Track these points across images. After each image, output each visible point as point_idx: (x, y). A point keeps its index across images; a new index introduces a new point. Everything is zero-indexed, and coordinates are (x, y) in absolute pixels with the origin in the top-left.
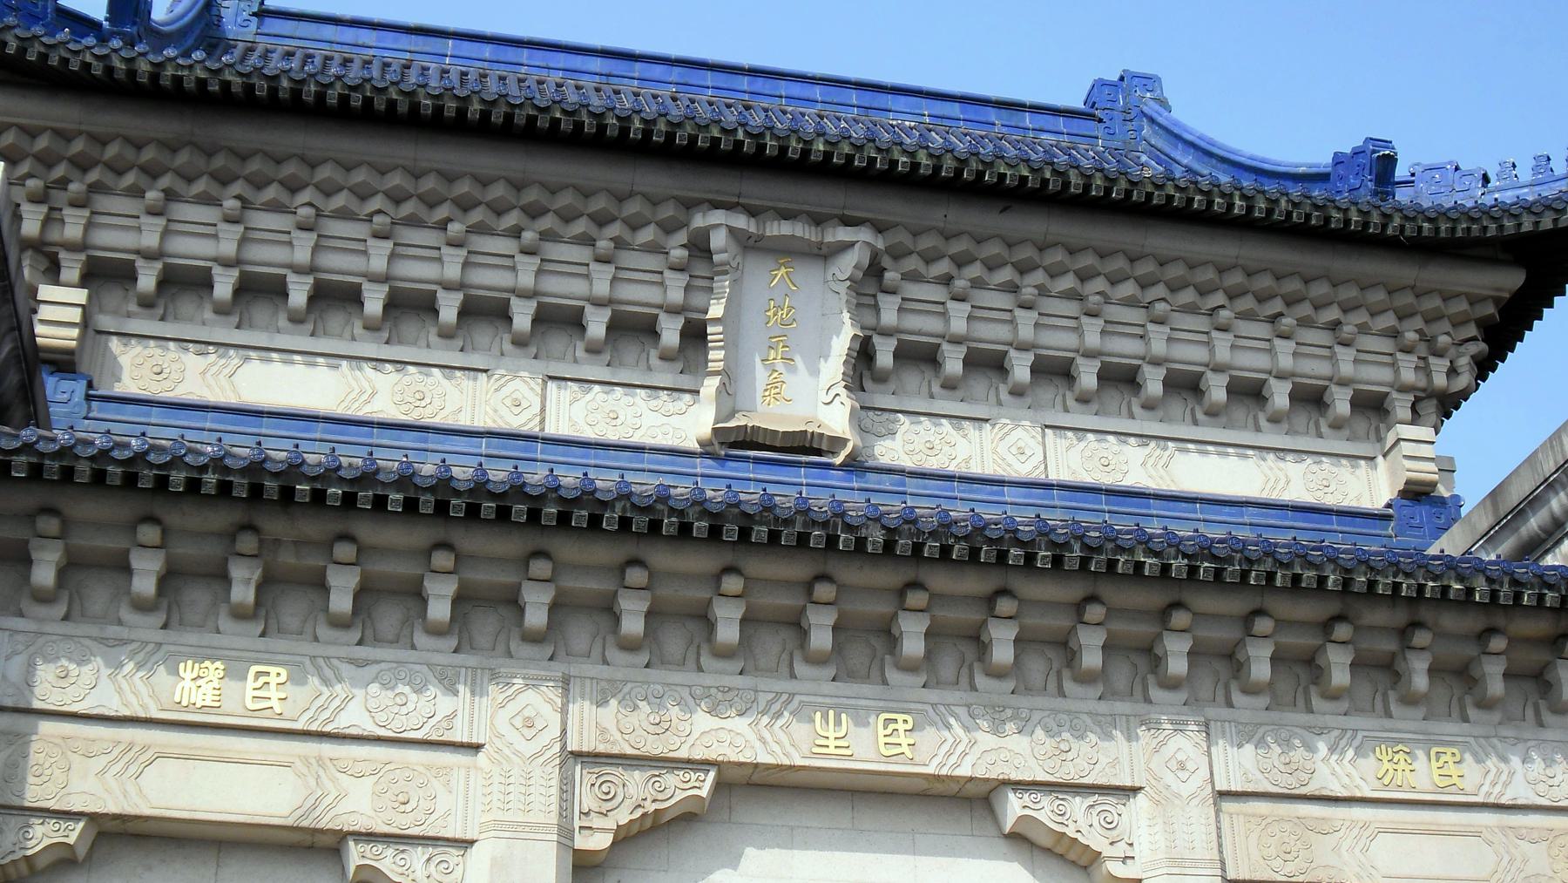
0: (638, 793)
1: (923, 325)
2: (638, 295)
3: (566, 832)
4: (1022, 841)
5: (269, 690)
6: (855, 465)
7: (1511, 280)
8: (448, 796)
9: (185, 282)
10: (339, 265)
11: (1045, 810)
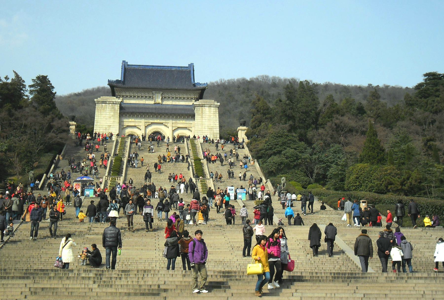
0: (148, 124)
1: (165, 96)
2: (150, 96)
4: (164, 125)
5: (133, 120)
8: (140, 124)
9: (127, 96)
10: (135, 95)
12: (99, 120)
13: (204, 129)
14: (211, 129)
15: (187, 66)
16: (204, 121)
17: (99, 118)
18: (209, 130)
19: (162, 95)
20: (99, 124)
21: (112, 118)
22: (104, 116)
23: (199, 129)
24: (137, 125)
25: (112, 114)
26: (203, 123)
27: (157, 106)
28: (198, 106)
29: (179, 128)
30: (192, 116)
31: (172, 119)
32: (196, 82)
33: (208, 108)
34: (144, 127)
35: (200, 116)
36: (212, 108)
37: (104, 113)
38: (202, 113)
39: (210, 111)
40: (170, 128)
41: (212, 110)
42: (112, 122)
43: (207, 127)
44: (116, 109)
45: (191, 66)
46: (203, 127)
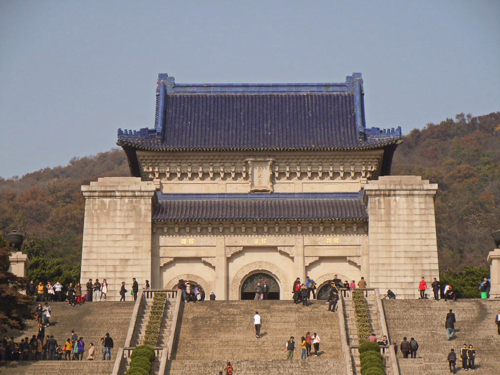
0: (234, 250)
3: (225, 255)
6: (272, 193)
7: (382, 152)
8: (212, 252)
11: (282, 249)
12: (95, 244)
13: (393, 261)
14: (415, 258)
15: (343, 81)
16: (393, 236)
17: (96, 238)
18: (408, 261)
19: (272, 167)
20: (94, 256)
21: (131, 237)
22: (109, 232)
23: (381, 261)
24: (201, 253)
25: (132, 225)
26: (393, 243)
27: (261, 199)
28: (376, 195)
29: (322, 259)
30: (361, 225)
31: (304, 232)
32: (369, 126)
33: (403, 199)
34: (223, 260)
35: (383, 224)
36: (416, 199)
37: (109, 225)
38: (388, 213)
39: (410, 209)
40: (299, 260)
41: (417, 205)
42: (131, 250)
43: (402, 255)
44: (143, 212)
45: (355, 80)
46: (393, 255)
